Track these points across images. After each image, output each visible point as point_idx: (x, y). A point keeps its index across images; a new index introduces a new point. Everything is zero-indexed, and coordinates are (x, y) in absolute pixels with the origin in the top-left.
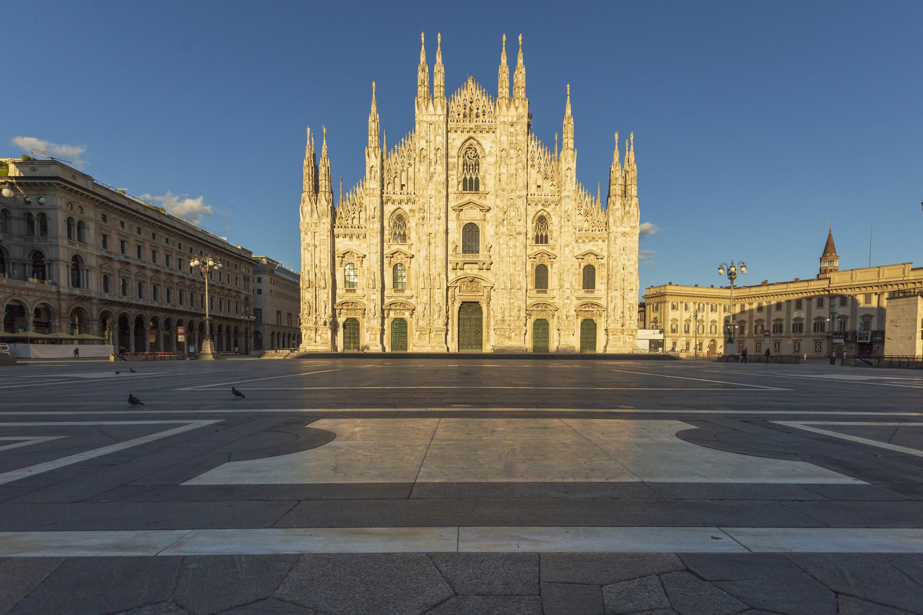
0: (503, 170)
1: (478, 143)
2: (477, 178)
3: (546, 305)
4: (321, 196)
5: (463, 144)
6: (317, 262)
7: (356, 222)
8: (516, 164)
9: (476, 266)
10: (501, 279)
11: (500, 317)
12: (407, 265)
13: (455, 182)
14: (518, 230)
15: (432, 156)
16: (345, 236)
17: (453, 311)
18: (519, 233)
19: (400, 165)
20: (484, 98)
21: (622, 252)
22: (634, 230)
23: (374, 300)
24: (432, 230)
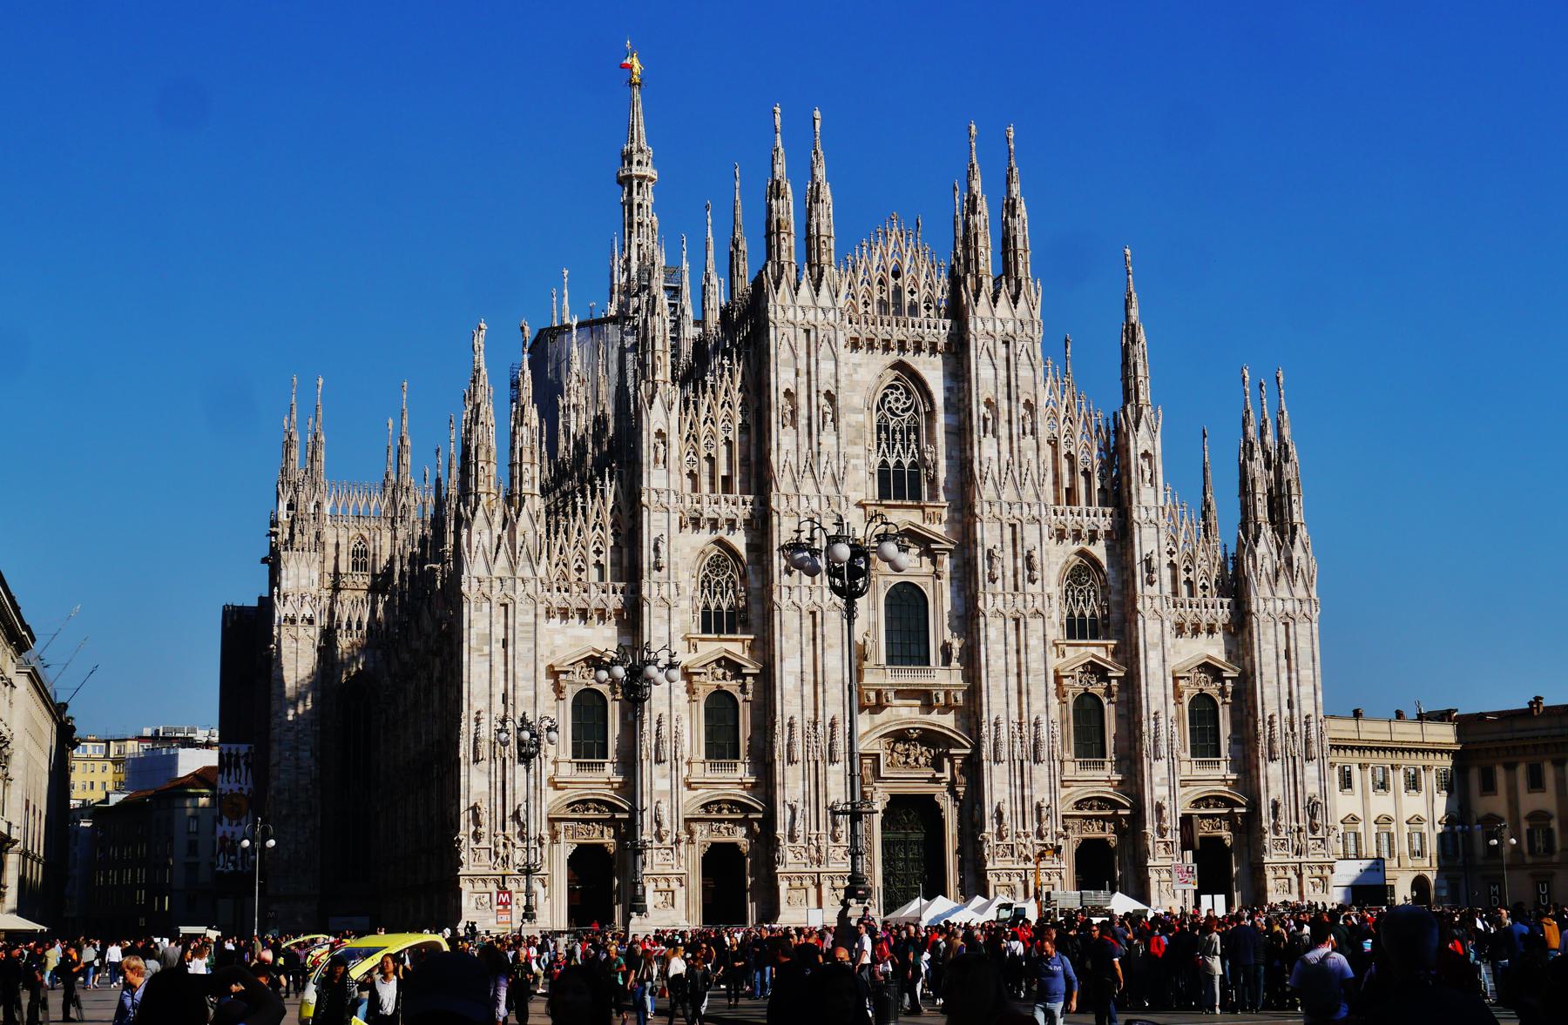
2: (913, 465)
13: (862, 474)
19: (720, 426)
21: (1283, 662)
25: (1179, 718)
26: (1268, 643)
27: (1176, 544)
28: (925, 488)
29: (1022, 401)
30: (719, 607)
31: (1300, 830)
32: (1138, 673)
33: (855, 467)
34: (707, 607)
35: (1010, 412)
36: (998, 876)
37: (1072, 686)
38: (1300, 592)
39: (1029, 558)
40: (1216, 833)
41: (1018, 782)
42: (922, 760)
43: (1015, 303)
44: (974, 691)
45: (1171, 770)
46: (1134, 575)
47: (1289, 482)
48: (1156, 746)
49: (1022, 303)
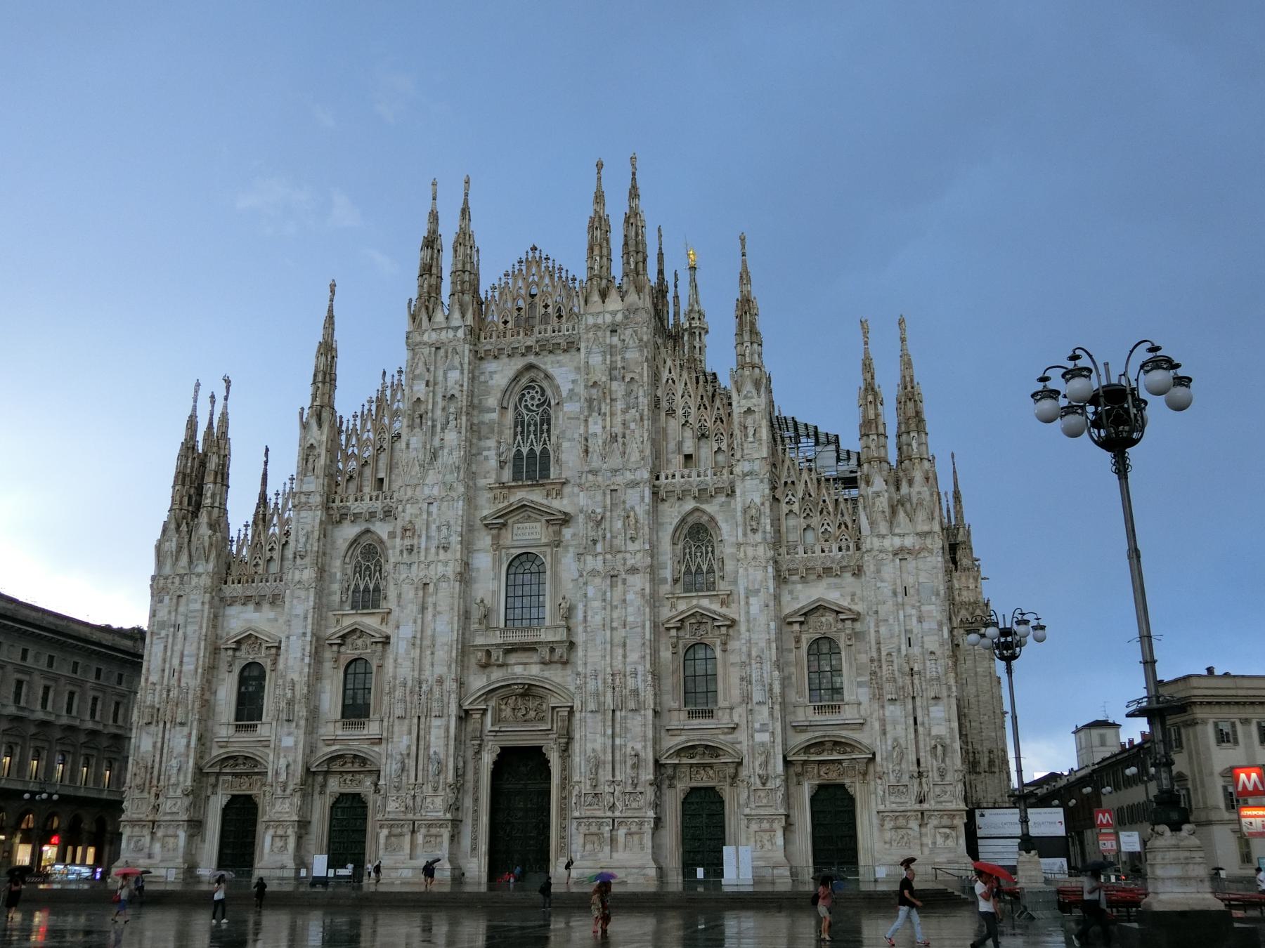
0: (595, 427)
1: (547, 376)
3: (713, 751)
4: (203, 518)
5: (516, 378)
7: (274, 567)
8: (624, 412)
9: (535, 658)
10: (591, 686)
11: (586, 787)
12: (374, 664)
13: (493, 463)
14: (630, 562)
15: (439, 412)
16: (247, 600)
17: (477, 771)
18: (633, 570)
22: (929, 541)
26: (882, 581)
28: (552, 469)
29: (627, 379)
30: (366, 589)
33: (487, 458)
34: (357, 586)
41: (609, 732)
42: (532, 714)
44: (572, 645)
45: (771, 714)
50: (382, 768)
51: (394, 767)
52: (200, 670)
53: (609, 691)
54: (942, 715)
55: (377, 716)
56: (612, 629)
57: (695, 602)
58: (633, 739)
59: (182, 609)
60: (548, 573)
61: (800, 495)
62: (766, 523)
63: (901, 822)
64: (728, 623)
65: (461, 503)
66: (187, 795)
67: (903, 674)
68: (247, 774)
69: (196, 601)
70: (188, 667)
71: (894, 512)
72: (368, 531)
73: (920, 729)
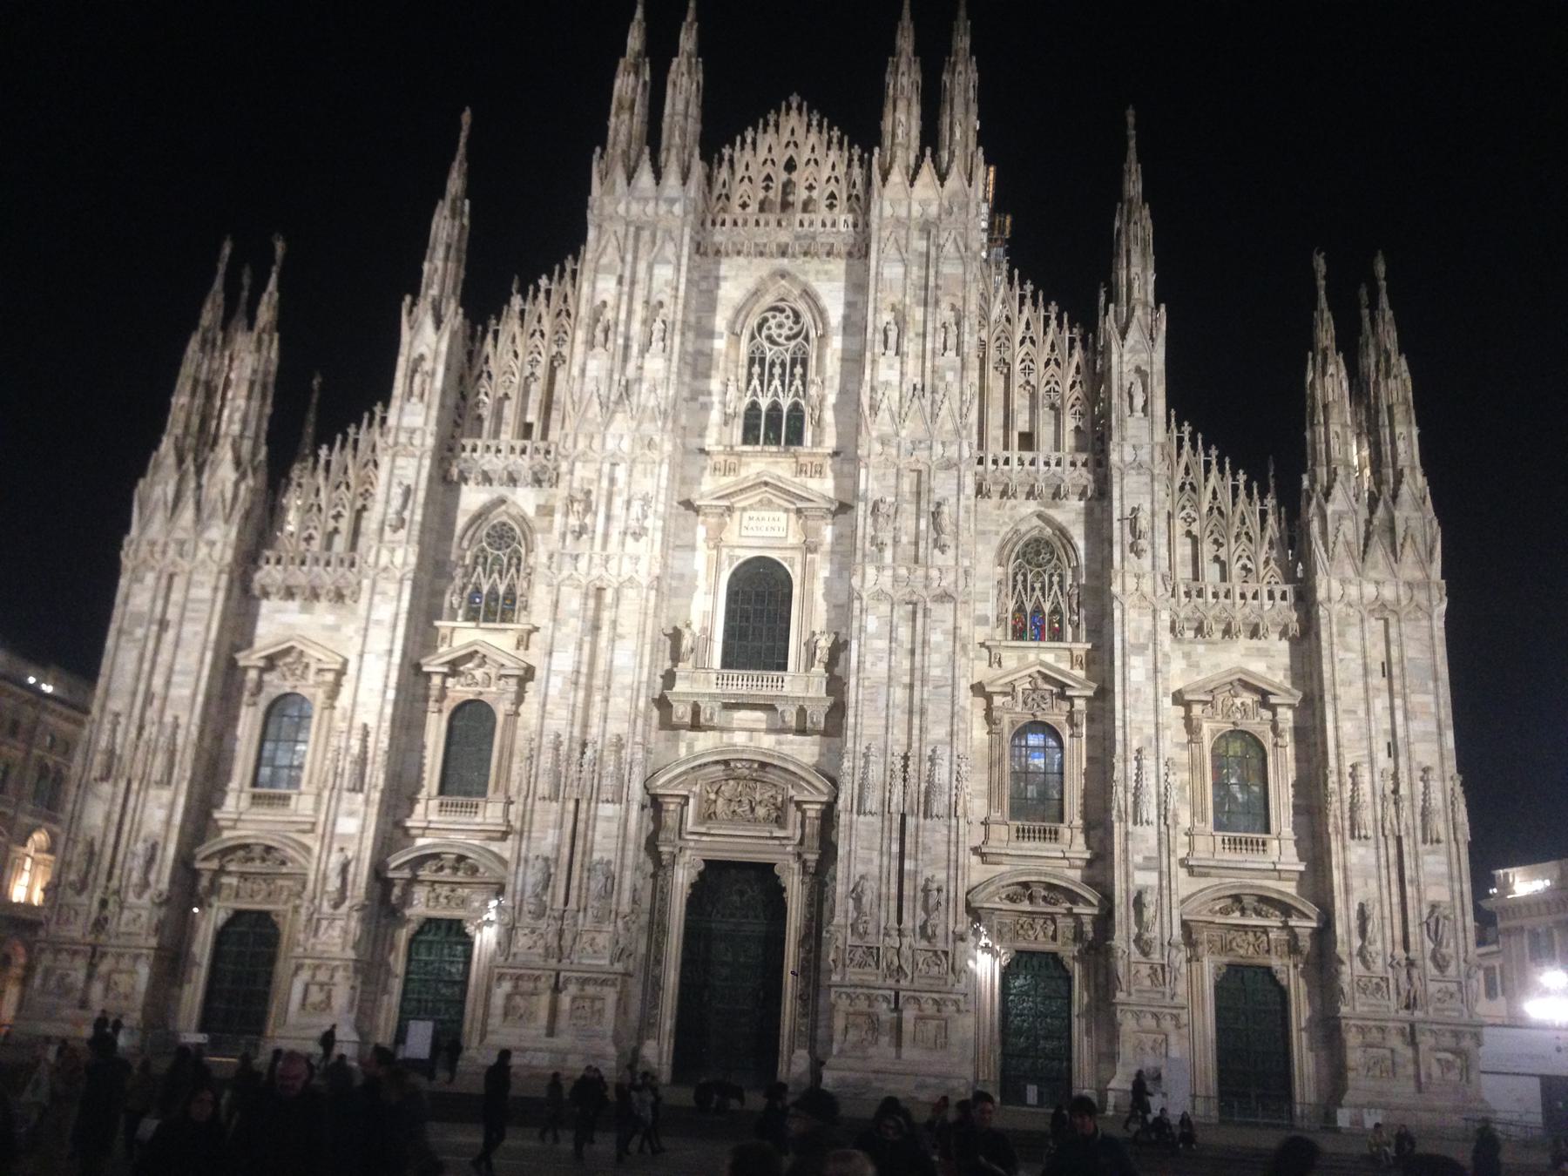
1: (808, 295)
2: (796, 407)
4: (225, 453)
5: (756, 294)
6: (158, 682)
7: (340, 543)
12: (502, 709)
13: (715, 416)
15: (636, 327)
16: (289, 594)
18: (945, 597)
20: (834, 155)
21: (1378, 681)
22: (1421, 596)
23: (349, 837)
24: (611, 579)
25: (1194, 766)
26: (1347, 649)
27: (1198, 510)
30: (493, 591)
31: (1411, 963)
32: (1113, 691)
35: (925, 322)
36: (848, 995)
37: (1009, 711)
38: (1409, 568)
39: (936, 515)
40: (1261, 960)
41: (895, 848)
42: (761, 811)
43: (942, 178)
45: (1164, 842)
46: (1111, 546)
47: (1390, 408)
48: (1136, 804)
49: (955, 181)
50: (512, 879)
51: (531, 880)
52: (200, 699)
53: (899, 781)
54: (1444, 869)
55: (501, 796)
56: (905, 686)
57: (1032, 657)
58: (933, 862)
59: (176, 596)
60: (796, 591)
61: (1205, 509)
62: (1162, 541)
63: (1375, 1036)
64: (1090, 693)
65: (665, 468)
66: (160, 905)
67: (1384, 797)
68: (267, 877)
69: (202, 584)
70: (182, 690)
71: (1366, 545)
72: (503, 501)
73: (1409, 890)
